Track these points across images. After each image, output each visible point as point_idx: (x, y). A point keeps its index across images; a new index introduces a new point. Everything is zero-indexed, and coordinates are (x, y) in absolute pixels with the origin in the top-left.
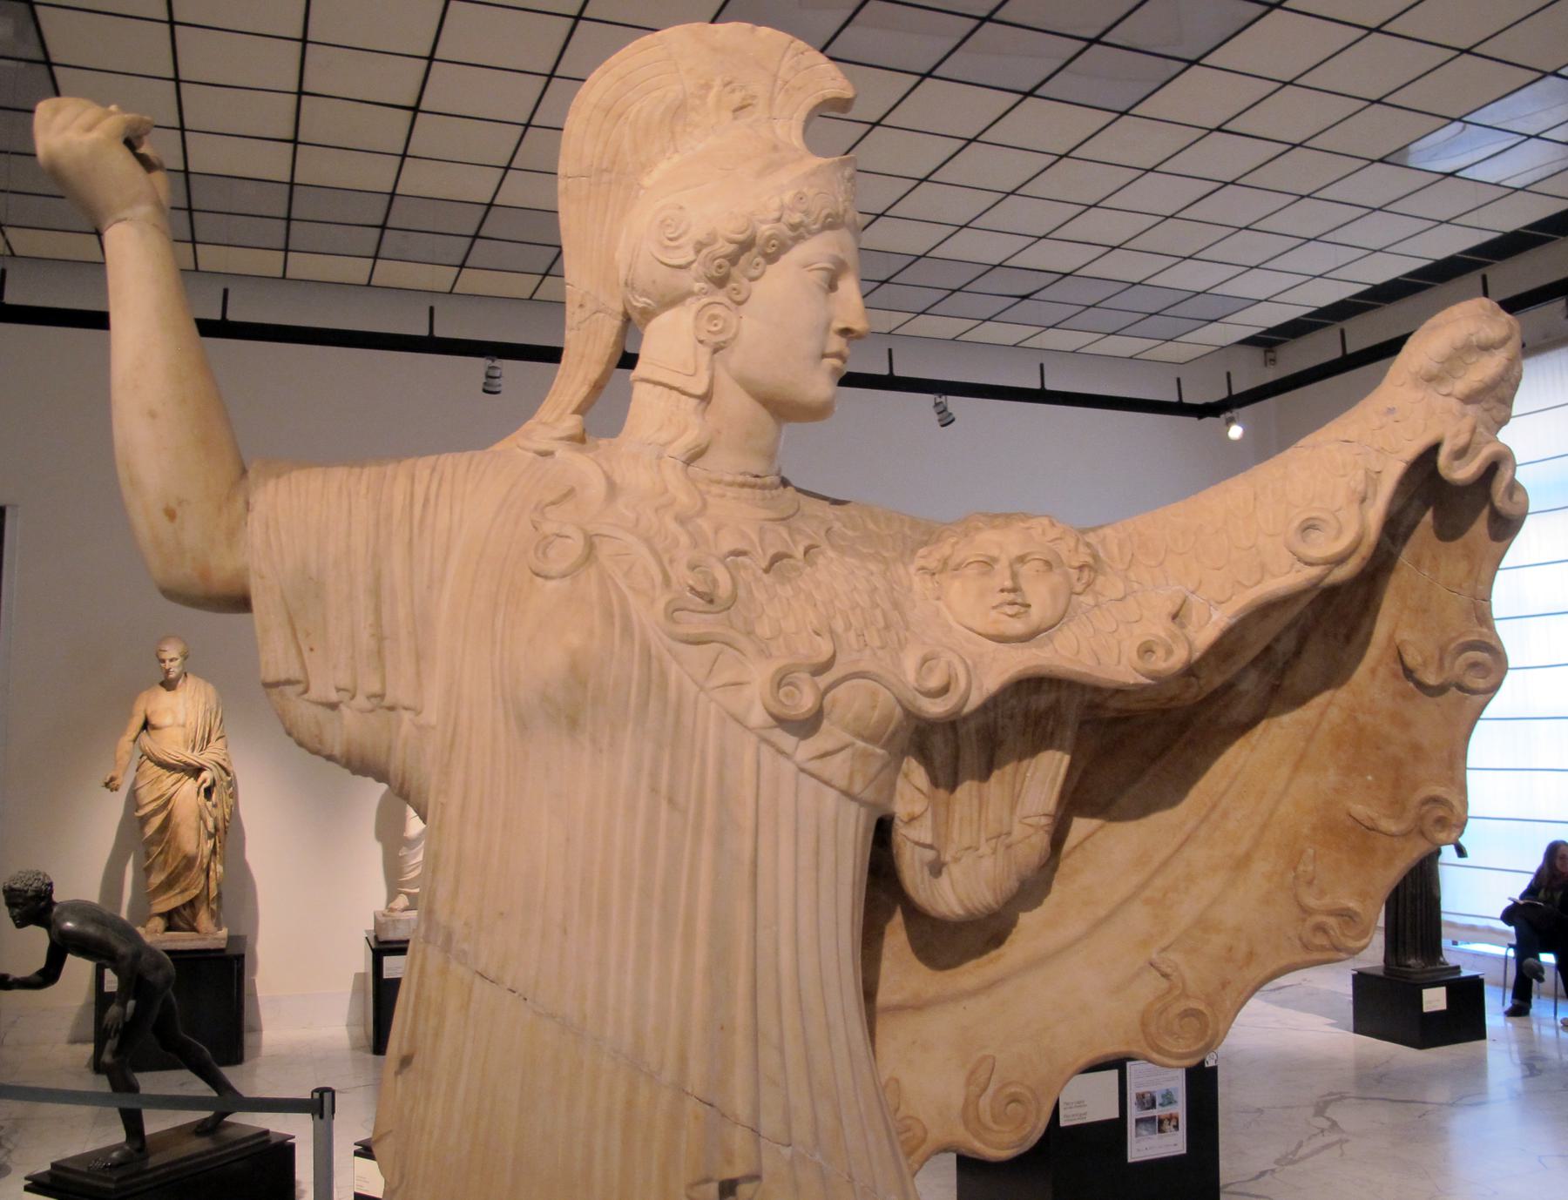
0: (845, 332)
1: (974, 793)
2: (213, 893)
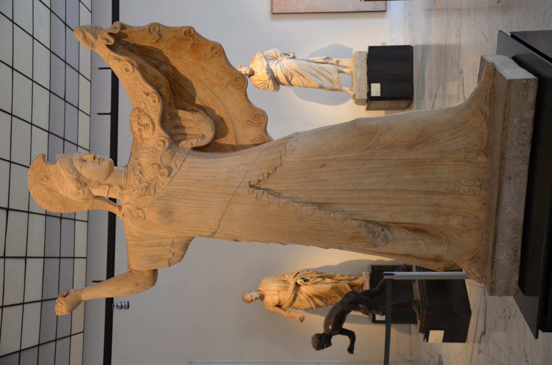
0: (94, 158)
2: (348, 277)
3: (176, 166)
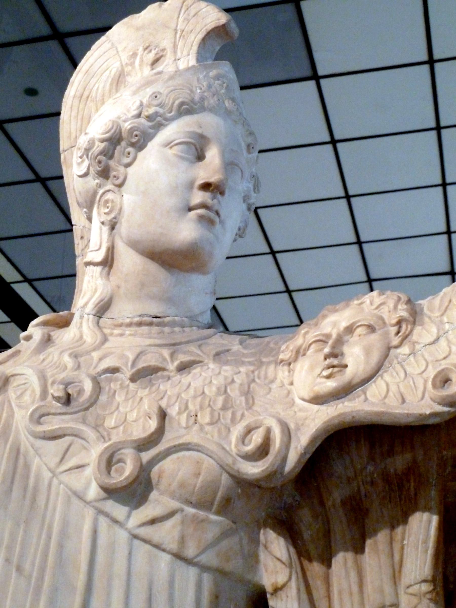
0: (206, 187)
1: (350, 563)
3: (153, 522)
